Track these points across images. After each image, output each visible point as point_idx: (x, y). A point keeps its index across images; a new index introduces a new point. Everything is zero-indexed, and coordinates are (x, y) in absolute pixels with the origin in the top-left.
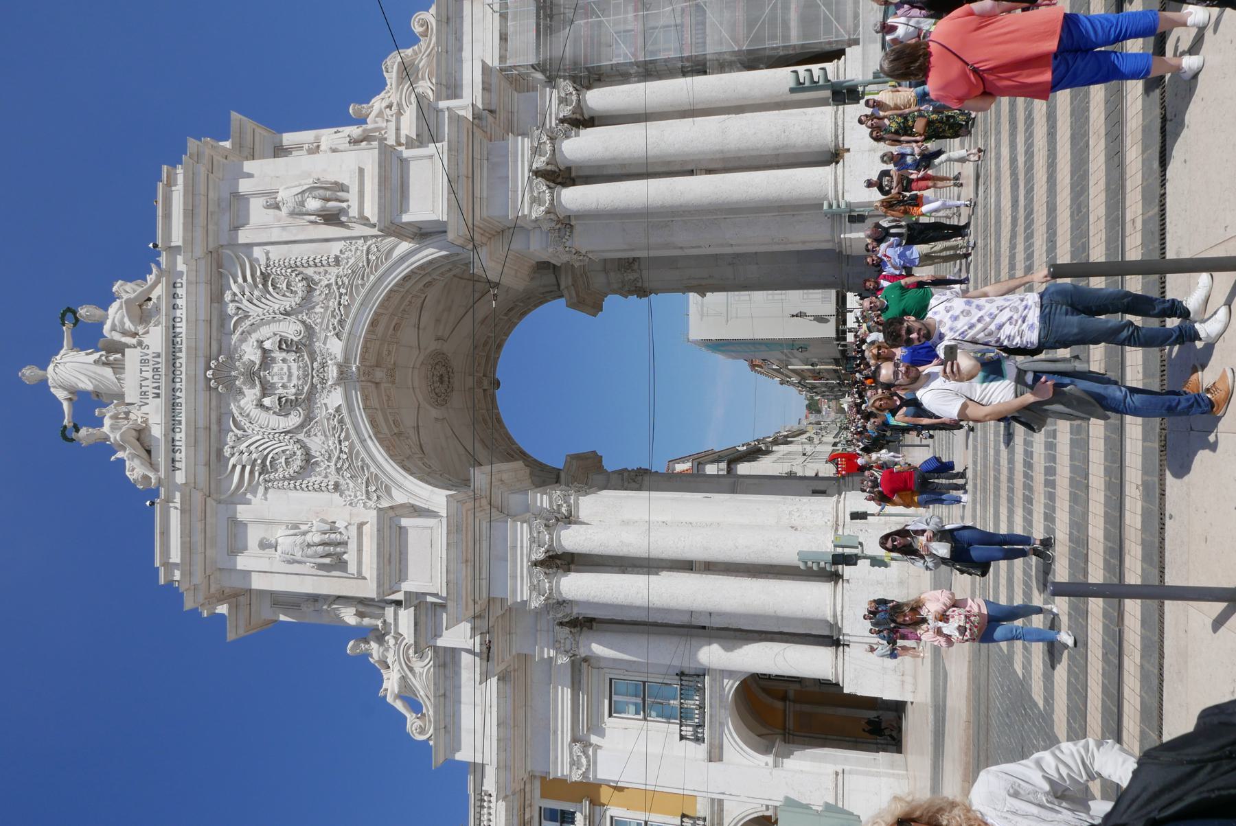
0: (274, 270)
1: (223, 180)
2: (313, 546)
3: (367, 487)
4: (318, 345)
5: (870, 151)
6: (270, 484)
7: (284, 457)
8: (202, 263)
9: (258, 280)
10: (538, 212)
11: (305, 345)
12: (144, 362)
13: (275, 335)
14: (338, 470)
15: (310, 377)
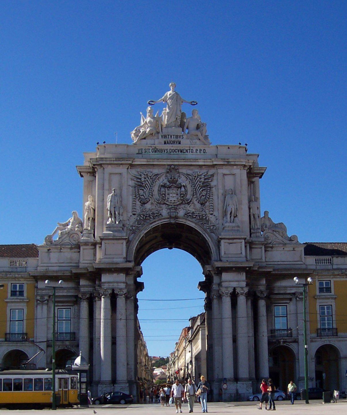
0: (208, 190)
1: (240, 170)
2: (114, 209)
3: (135, 226)
4: (183, 206)
5: (237, 389)
6: (134, 189)
7: (143, 194)
8: (211, 164)
9: (205, 184)
10: (223, 290)
11: (182, 202)
12: (177, 137)
13: (186, 191)
14: (140, 215)
15: (172, 204)
